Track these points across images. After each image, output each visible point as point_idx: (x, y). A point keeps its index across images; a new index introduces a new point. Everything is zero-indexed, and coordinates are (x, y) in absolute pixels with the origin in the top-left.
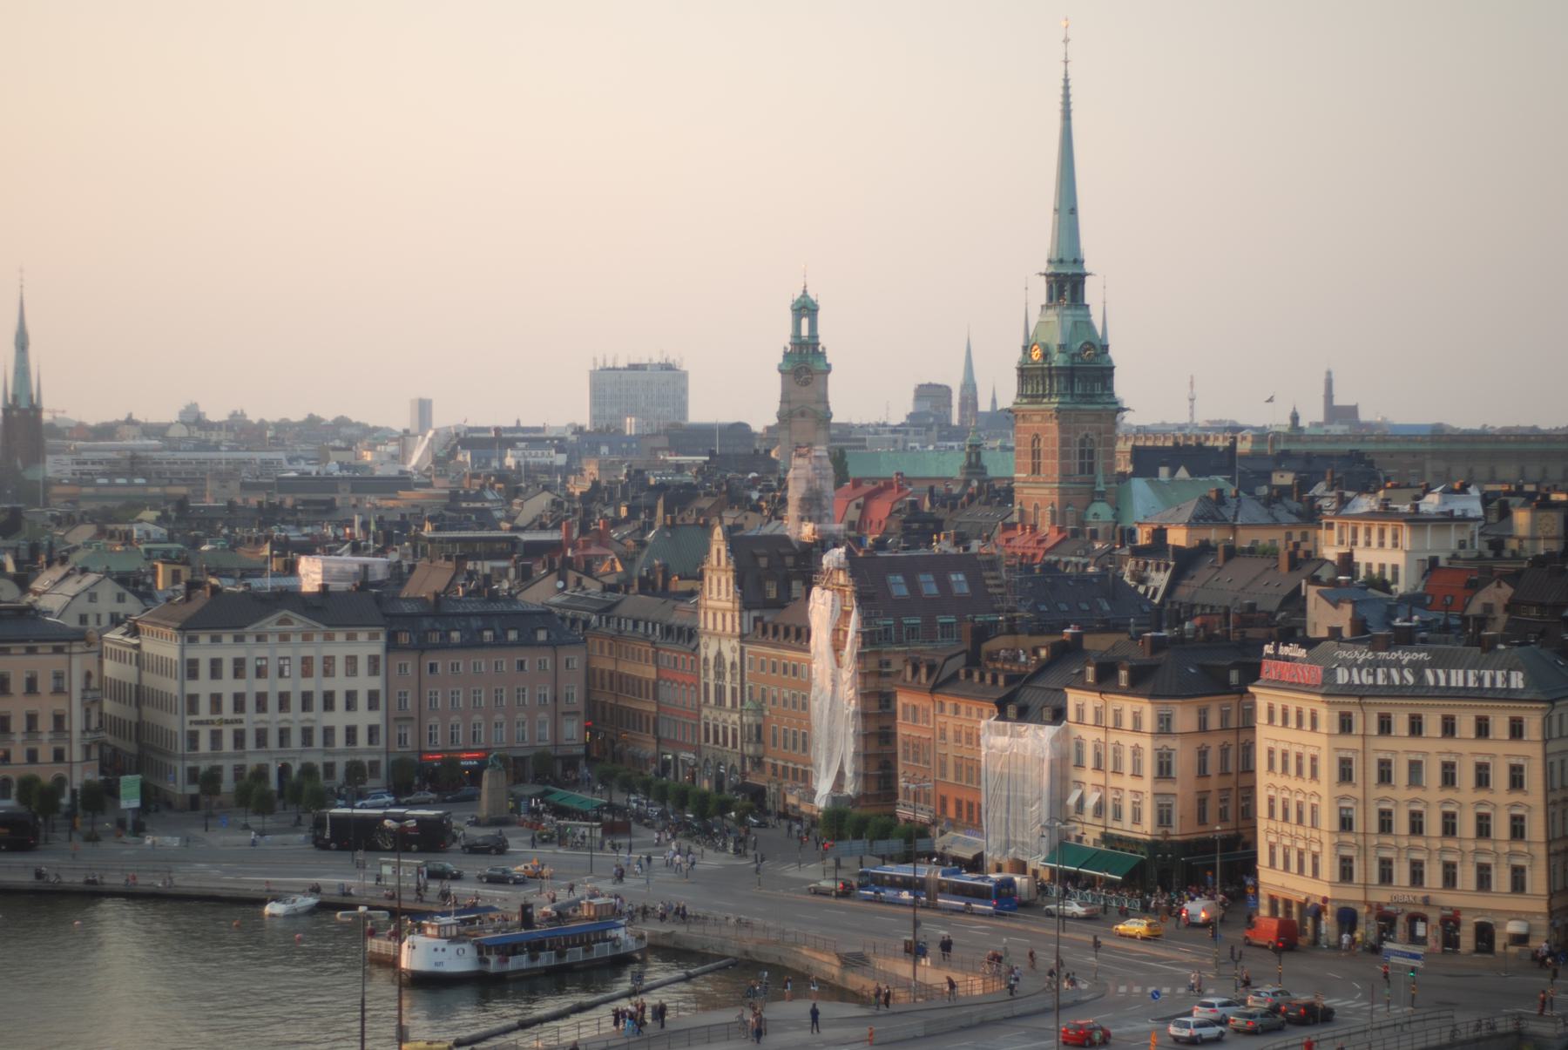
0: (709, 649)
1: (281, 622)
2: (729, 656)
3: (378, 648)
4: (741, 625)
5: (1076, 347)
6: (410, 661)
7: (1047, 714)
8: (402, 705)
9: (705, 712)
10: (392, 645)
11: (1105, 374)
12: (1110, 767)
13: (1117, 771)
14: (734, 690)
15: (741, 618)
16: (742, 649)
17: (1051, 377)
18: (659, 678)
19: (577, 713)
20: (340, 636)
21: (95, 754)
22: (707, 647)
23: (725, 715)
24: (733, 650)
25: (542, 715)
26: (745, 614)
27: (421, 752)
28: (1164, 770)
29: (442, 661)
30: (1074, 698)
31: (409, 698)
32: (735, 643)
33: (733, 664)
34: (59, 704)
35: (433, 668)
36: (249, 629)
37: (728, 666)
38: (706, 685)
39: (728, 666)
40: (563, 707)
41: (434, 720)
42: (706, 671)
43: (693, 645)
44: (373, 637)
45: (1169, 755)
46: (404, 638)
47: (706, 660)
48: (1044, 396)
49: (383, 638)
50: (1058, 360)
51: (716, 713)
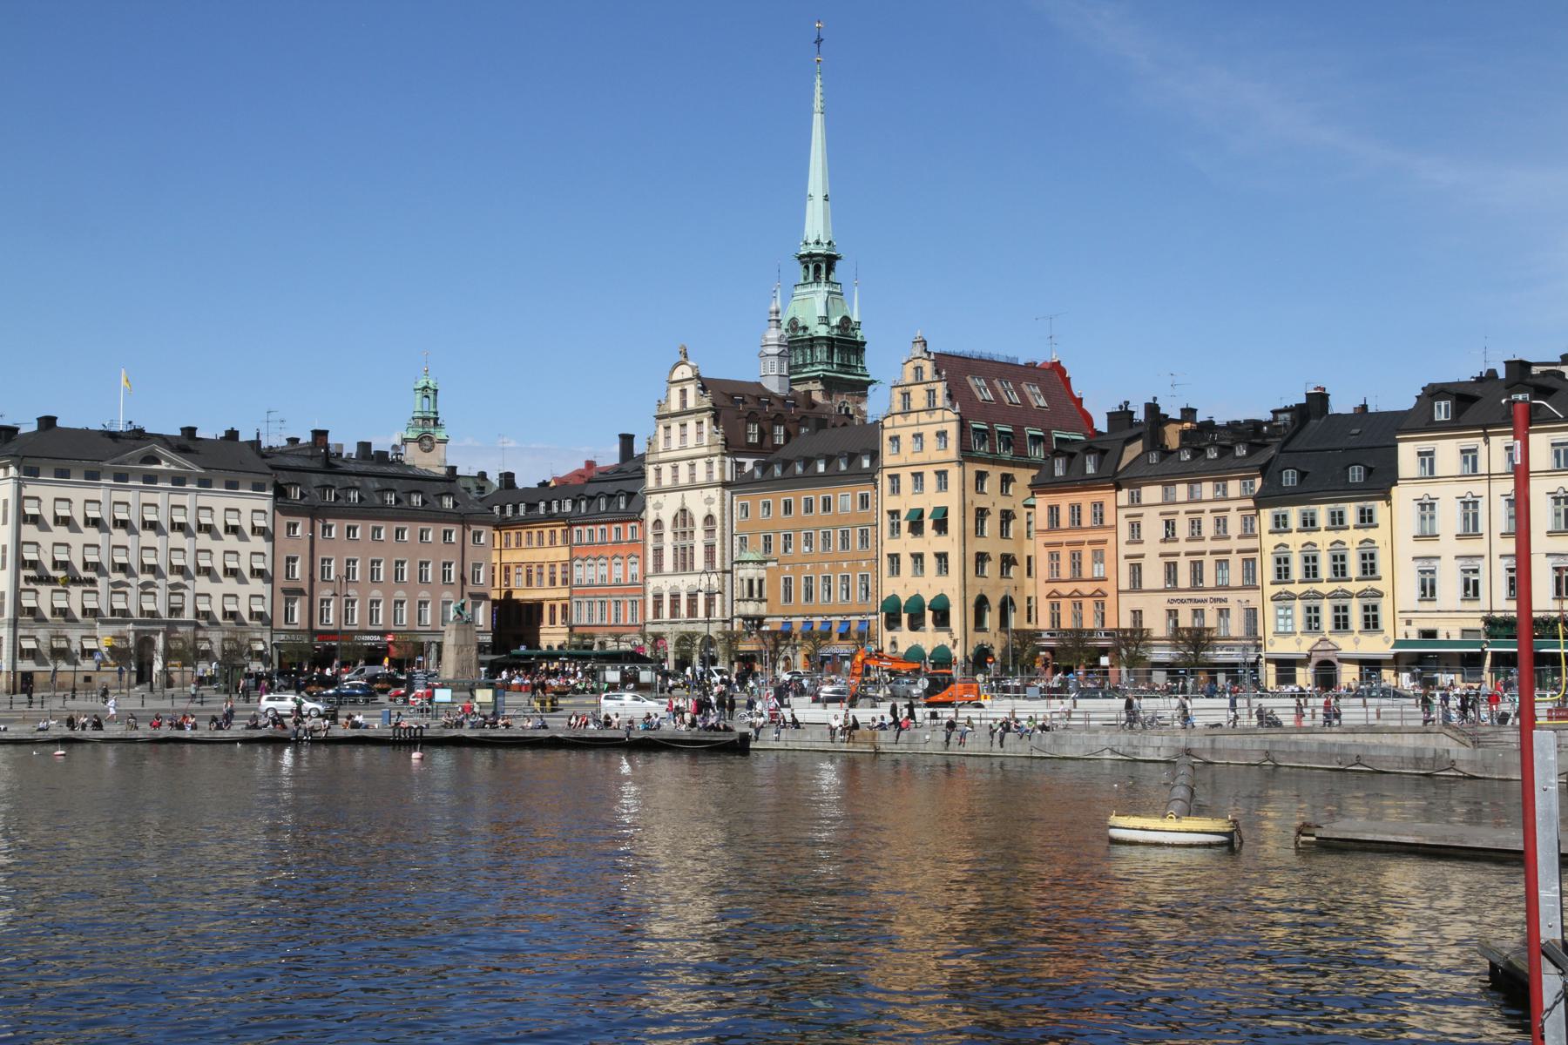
0: (660, 507)
3: (266, 504)
4: (722, 470)
5: (835, 321)
7: (1356, 474)
9: (654, 583)
11: (859, 348)
14: (710, 548)
15: (723, 462)
16: (723, 499)
17: (812, 347)
18: (571, 560)
22: (658, 506)
24: (709, 501)
25: (447, 595)
26: (728, 460)
27: (312, 632)
31: (298, 564)
33: (709, 519)
37: (699, 522)
38: (658, 552)
39: (699, 522)
42: (659, 536)
43: (634, 507)
44: (258, 487)
46: (295, 493)
47: (658, 523)
48: (805, 365)
50: (822, 331)
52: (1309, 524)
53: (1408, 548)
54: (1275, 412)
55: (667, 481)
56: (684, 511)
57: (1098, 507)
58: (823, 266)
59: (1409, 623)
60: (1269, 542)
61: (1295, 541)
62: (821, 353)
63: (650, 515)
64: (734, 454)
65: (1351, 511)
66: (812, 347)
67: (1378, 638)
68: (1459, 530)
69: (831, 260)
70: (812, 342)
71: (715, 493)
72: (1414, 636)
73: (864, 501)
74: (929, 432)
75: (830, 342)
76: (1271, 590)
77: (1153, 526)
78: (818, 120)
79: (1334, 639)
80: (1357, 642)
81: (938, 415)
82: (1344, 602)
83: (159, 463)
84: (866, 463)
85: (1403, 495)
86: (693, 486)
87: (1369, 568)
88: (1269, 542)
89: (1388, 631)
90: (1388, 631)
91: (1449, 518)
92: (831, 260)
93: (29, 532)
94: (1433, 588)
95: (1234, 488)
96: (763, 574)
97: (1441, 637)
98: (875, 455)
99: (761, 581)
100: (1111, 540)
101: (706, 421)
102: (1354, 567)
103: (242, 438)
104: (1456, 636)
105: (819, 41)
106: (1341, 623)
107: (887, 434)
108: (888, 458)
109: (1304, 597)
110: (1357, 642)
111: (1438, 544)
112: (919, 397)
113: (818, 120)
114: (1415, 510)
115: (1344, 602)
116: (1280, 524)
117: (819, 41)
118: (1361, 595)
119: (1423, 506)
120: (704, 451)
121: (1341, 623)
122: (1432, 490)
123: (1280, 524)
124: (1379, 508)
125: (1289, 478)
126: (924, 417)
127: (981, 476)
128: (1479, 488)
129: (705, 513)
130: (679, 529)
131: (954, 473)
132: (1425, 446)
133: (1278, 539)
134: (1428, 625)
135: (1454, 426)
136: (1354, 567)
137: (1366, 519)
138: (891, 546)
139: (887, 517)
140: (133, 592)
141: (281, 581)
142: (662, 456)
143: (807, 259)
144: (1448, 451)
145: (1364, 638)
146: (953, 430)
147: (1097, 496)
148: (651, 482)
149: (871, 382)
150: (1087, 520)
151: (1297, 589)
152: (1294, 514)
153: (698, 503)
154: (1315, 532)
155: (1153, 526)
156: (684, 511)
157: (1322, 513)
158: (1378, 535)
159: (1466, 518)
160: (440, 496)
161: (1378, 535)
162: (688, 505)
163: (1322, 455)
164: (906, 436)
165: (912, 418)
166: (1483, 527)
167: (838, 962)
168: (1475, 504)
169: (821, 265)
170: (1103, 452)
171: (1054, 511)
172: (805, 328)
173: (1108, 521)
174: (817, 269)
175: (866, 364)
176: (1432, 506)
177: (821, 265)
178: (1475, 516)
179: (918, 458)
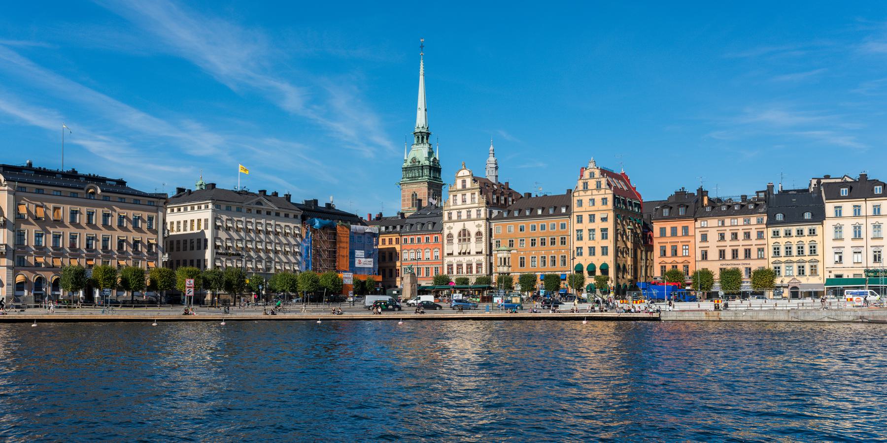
5: (432, 159)
7: (807, 216)
9: (447, 260)
12: (871, 234)
30: (830, 208)
32: (482, 223)
33: (479, 234)
37: (473, 235)
39: (473, 235)
47: (450, 236)
50: (427, 163)
52: (788, 234)
53: (830, 243)
54: (757, 192)
55: (454, 216)
56: (464, 230)
57: (686, 229)
59: (830, 272)
60: (771, 241)
61: (782, 241)
62: (426, 172)
63: (446, 232)
65: (806, 229)
67: (817, 277)
68: (853, 236)
69: (428, 134)
72: (833, 277)
73: (563, 226)
74: (598, 199)
75: (430, 168)
76: (772, 260)
77: (713, 236)
78: (421, 78)
79: (798, 278)
80: (808, 279)
81: (602, 191)
82: (803, 264)
84: (564, 210)
85: (829, 224)
86: (469, 218)
87: (813, 251)
88: (771, 241)
89: (821, 275)
90: (821, 275)
91: (848, 232)
94: (879, 257)
95: (753, 220)
96: (510, 255)
97: (845, 277)
98: (568, 207)
100: (692, 241)
101: (477, 193)
102: (807, 250)
103: (279, 196)
104: (851, 277)
105: (422, 47)
106: (801, 272)
108: (575, 208)
109: (798, 262)
110: (808, 279)
111: (847, 241)
112: (592, 184)
113: (421, 78)
114: (832, 230)
115: (803, 264)
116: (776, 234)
117: (422, 47)
118: (810, 261)
119: (836, 228)
120: (476, 205)
121: (801, 272)
122: (840, 221)
123: (776, 234)
124: (818, 228)
125: (779, 217)
126: (595, 192)
128: (862, 221)
129: (476, 230)
130: (462, 238)
132: (877, 203)
133: (775, 240)
134: (839, 273)
135: (851, 196)
136: (807, 250)
137: (812, 232)
138: (578, 244)
139: (575, 232)
144: (848, 207)
145: (811, 278)
146: (610, 198)
147: (685, 223)
148: (446, 218)
150: (679, 233)
151: (795, 259)
152: (782, 230)
153: (472, 228)
154: (790, 237)
155: (713, 236)
156: (464, 230)
157: (794, 230)
159: (855, 232)
162: (466, 227)
163: (796, 207)
164: (586, 201)
165: (589, 193)
166: (863, 235)
167: (626, 407)
168: (860, 227)
169: (424, 136)
170: (687, 207)
171: (663, 231)
173: (691, 233)
174: (423, 138)
175: (442, 176)
176: (841, 228)
177: (424, 136)
178: (860, 232)
179: (593, 208)
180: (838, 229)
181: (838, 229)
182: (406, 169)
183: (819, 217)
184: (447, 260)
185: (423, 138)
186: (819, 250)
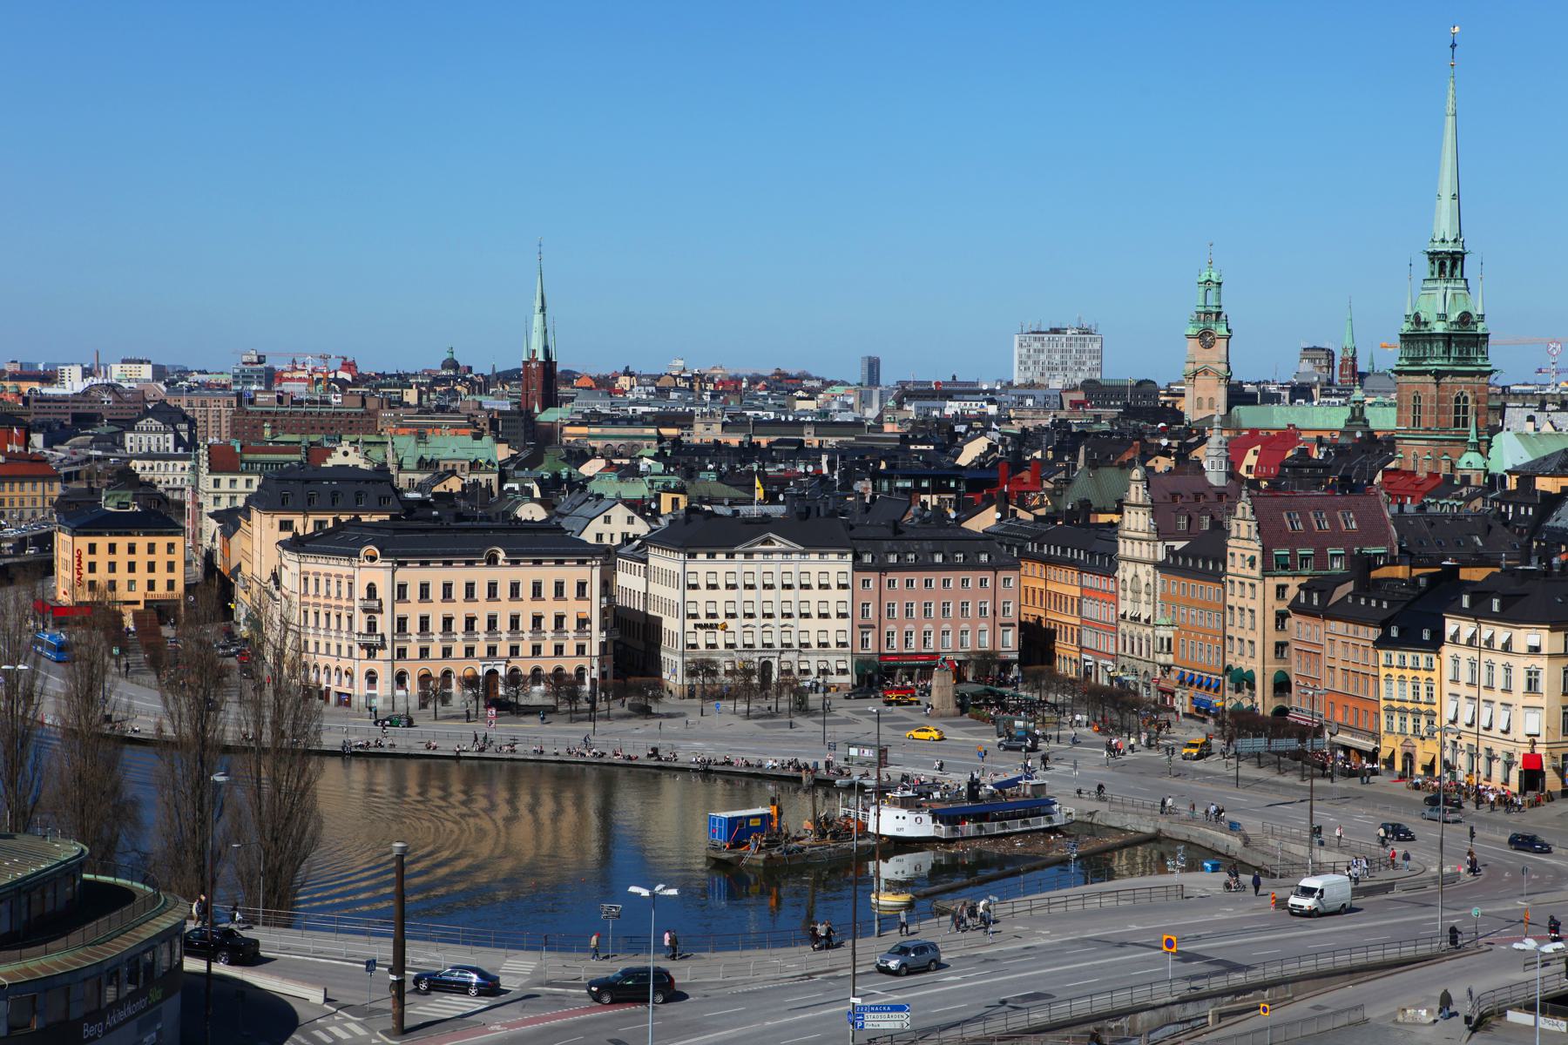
0: (1126, 572)
1: (765, 542)
2: (1143, 579)
3: (848, 567)
5: (1454, 317)
6: (873, 577)
7: (1426, 636)
8: (865, 613)
9: (1123, 625)
10: (858, 566)
12: (1484, 682)
13: (1490, 687)
17: (1431, 343)
19: (1013, 625)
20: (815, 557)
21: (610, 649)
23: (1140, 629)
24: (1148, 574)
27: (882, 656)
28: (1532, 686)
29: (899, 578)
34: (583, 607)
35: (891, 583)
36: (739, 548)
40: (1001, 619)
41: (891, 627)
45: (1537, 673)
46: (867, 559)
48: (1425, 359)
49: (850, 557)
50: (1439, 328)
51: (1132, 627)
58: (1448, 263)
62: (1439, 349)
63: (1120, 574)
64: (1164, 541)
66: (1431, 343)
69: (1457, 258)
70: (1431, 338)
71: (1150, 567)
75: (1448, 339)
76: (1383, 704)
83: (772, 543)
92: (1457, 258)
93: (691, 594)
96: (1171, 634)
99: (1169, 640)
105: (1453, 46)
107: (1230, 550)
117: (1453, 46)
125: (1394, 633)
127: (1281, 590)
128: (1475, 654)
131: (1259, 586)
140: (757, 631)
141: (859, 620)
142: (1127, 533)
143: (1433, 256)
149: (1491, 372)
152: (1396, 655)
158: (1435, 676)
160: (978, 554)
161: (1435, 676)
169: (1448, 263)
172: (1426, 324)
174: (1442, 265)
180: (1456, 660)
181: (1456, 660)
182: (1407, 339)
183: (1436, 643)
184: (1123, 625)
185: (1442, 265)
186: (1436, 699)
